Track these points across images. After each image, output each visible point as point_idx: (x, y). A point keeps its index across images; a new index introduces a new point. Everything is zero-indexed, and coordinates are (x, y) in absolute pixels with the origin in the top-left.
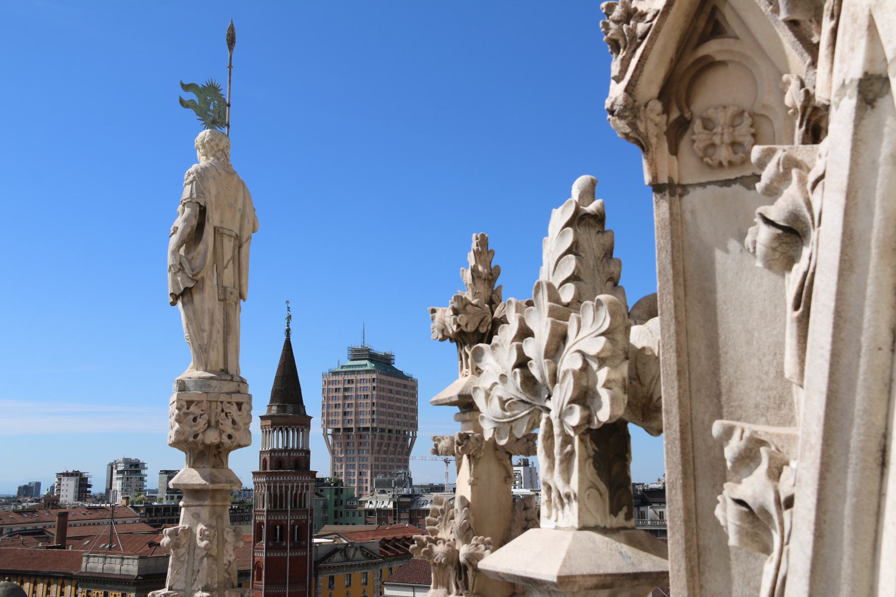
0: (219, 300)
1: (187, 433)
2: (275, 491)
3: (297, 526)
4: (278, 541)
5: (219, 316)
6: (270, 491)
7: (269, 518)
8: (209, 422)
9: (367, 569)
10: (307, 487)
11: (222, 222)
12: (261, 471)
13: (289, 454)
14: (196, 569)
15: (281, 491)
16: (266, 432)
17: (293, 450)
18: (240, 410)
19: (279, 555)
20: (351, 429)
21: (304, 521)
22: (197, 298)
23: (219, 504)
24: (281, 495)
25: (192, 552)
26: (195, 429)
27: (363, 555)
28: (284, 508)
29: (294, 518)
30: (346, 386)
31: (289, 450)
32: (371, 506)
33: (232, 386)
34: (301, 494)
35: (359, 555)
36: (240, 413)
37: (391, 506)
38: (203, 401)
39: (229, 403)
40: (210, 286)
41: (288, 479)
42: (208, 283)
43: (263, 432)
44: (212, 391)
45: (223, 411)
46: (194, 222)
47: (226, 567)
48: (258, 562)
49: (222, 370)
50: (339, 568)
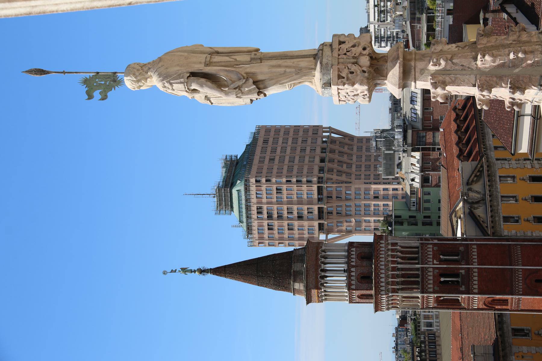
0: (261, 62)
1: (362, 78)
2: (397, 283)
3: (441, 257)
4: (459, 279)
5: (274, 62)
6: (398, 289)
7: (431, 290)
8: (353, 63)
9: (495, 176)
10: (394, 244)
11: (201, 63)
12: (373, 301)
13: (353, 266)
14: (461, 68)
15: (398, 276)
16: (326, 295)
17: (348, 263)
18: (344, 42)
19: (476, 278)
20: (320, 210)
21: (435, 248)
22: (260, 77)
23: (414, 56)
24: (403, 276)
25: (449, 72)
26: (359, 72)
27: (477, 181)
28: (419, 273)
29: (431, 260)
30: (265, 216)
31: (348, 266)
32: (418, 179)
33: (327, 51)
34: (402, 252)
35: (477, 187)
36: (347, 42)
37: (417, 155)
38: (338, 68)
39: (339, 50)
40: (249, 68)
41: (383, 267)
42: (248, 70)
43: (326, 299)
44: (330, 62)
45: (345, 54)
46: (203, 80)
47: (460, 49)
48: (485, 305)
49: (315, 58)
50: (494, 211)
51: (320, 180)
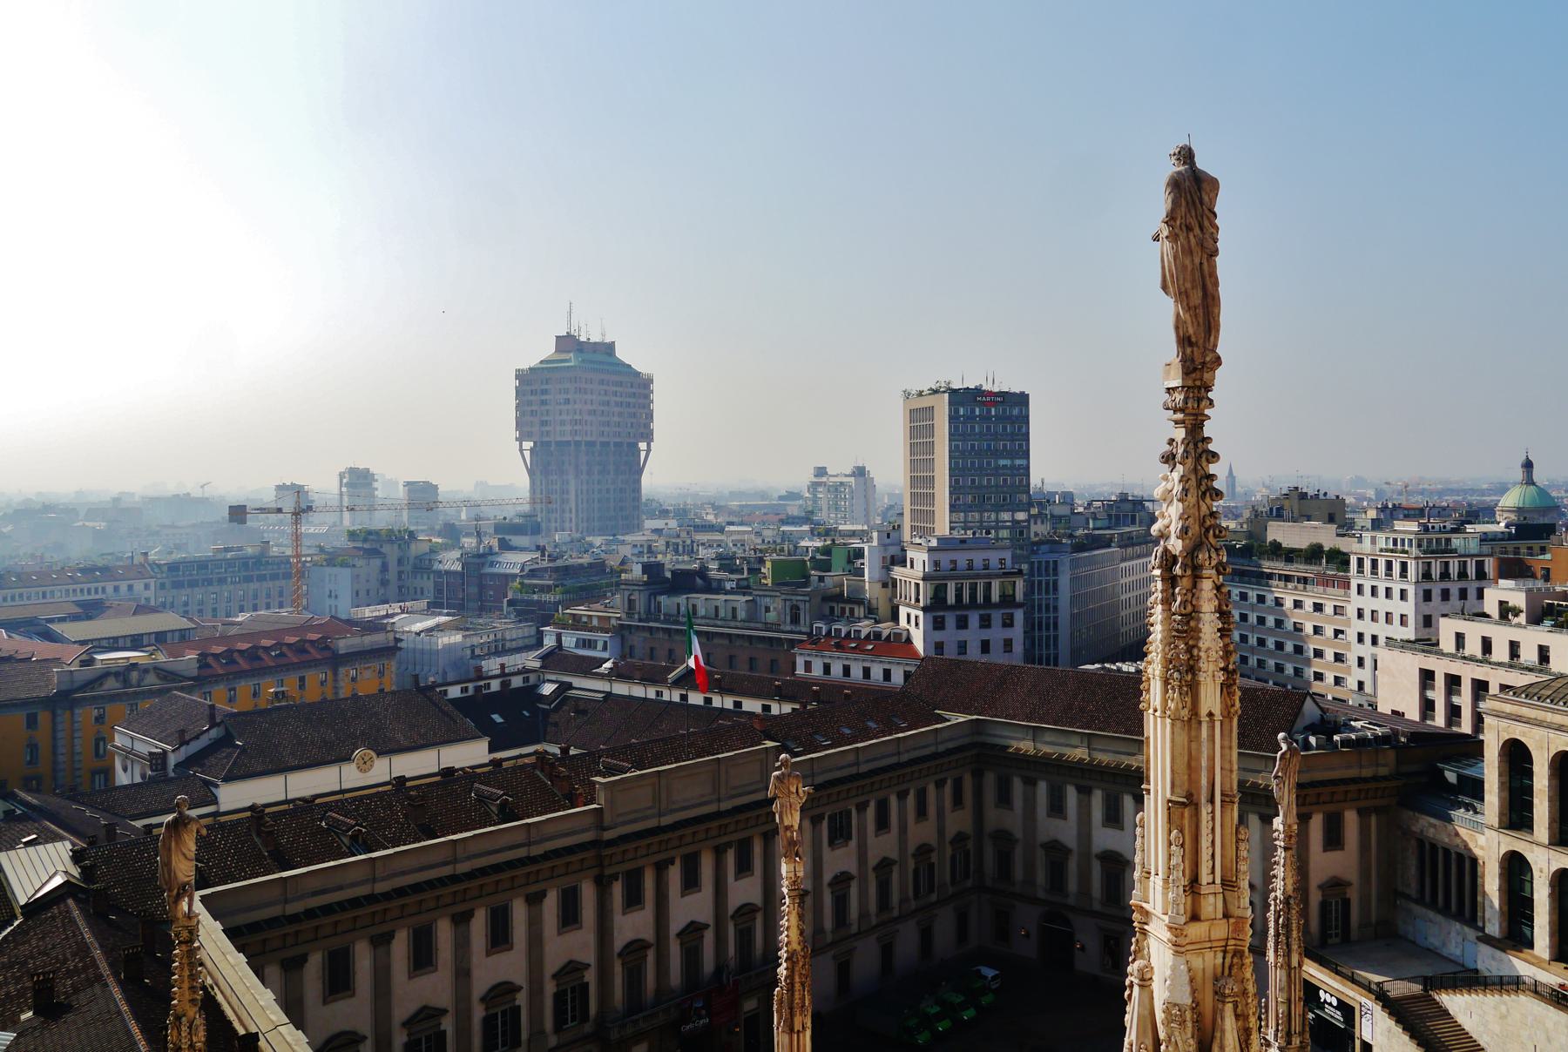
20: (548, 444)
27: (158, 676)
32: (441, 567)
35: (151, 679)
37: (460, 569)
50: (113, 698)
51: (578, 444)
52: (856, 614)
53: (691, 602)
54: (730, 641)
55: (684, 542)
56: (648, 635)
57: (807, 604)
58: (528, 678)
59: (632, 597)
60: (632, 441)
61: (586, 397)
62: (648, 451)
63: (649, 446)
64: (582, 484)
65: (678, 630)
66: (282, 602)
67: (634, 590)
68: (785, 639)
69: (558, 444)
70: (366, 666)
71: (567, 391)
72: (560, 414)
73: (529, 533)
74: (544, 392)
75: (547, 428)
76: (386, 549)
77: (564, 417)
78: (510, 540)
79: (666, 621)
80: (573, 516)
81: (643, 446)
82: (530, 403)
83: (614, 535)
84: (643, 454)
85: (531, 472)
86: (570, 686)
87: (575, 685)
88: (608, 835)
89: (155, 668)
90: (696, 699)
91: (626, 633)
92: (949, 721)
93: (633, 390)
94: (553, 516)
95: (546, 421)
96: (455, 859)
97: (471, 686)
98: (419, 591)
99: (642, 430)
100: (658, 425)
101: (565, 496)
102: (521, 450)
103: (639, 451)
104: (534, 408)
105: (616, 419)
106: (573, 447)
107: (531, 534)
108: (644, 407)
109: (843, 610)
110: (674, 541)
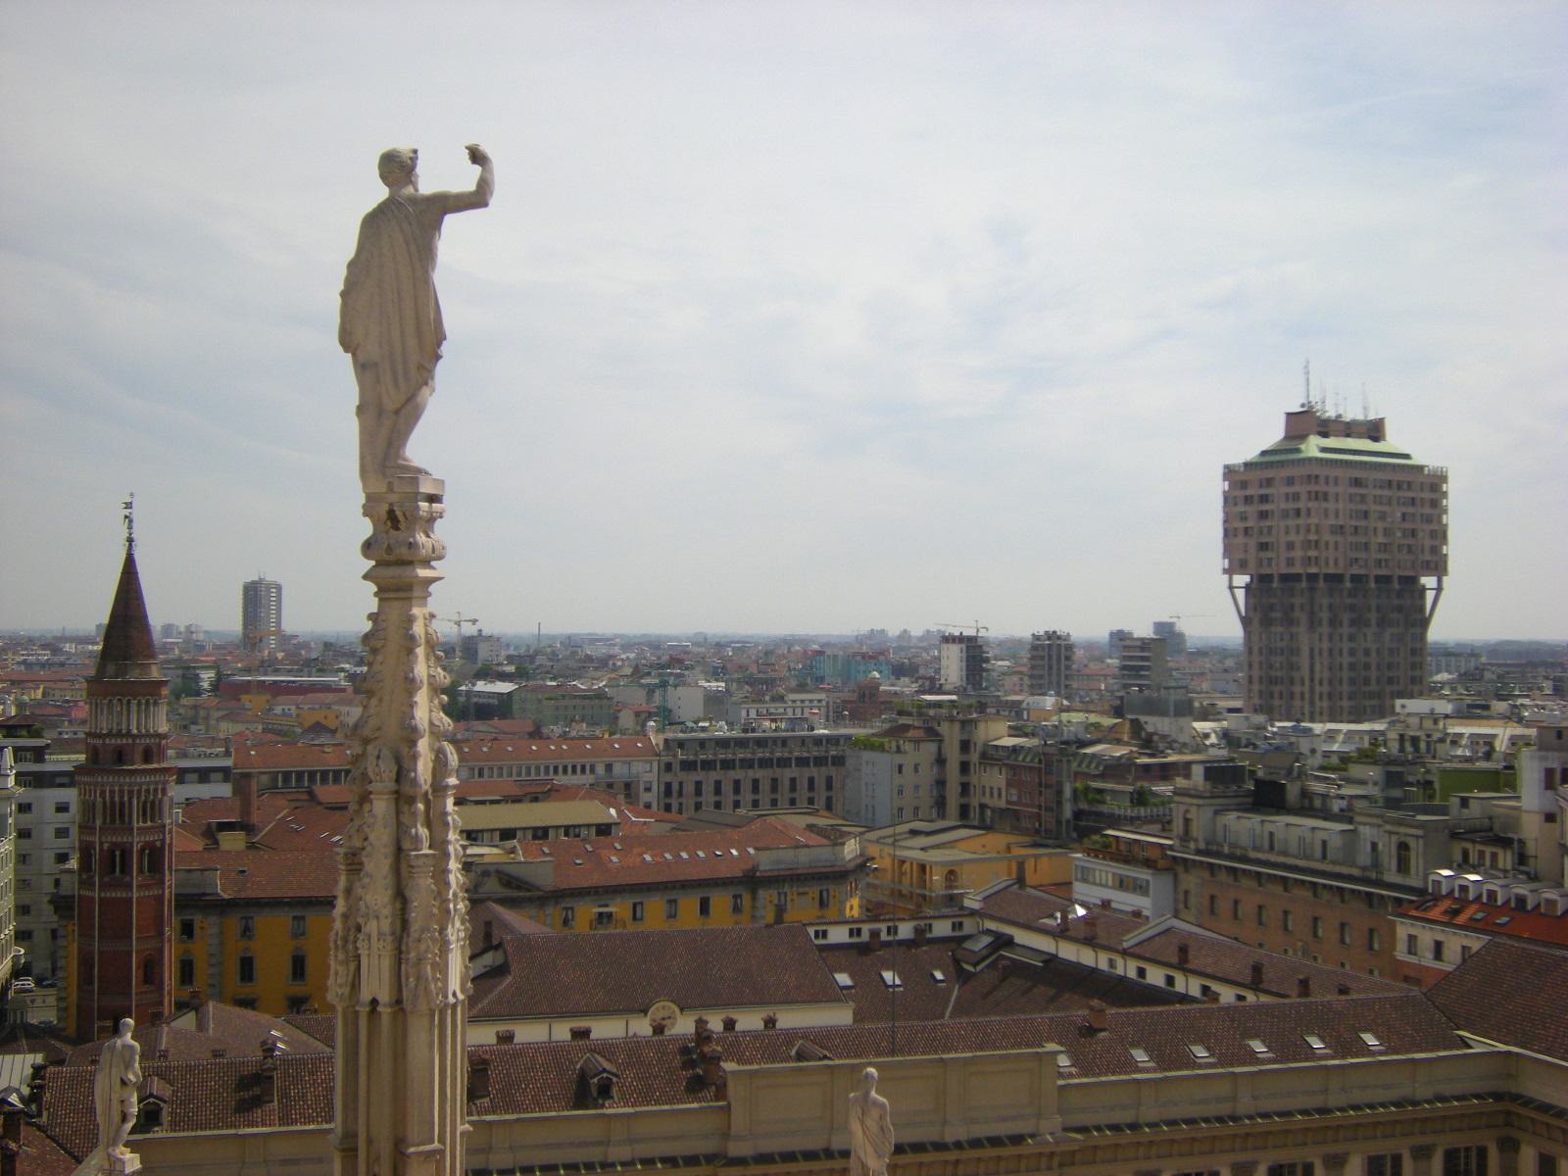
3: (147, 852)
6: (104, 798)
20: (1271, 576)
24: (122, 804)
34: (153, 802)
51: (1312, 577)
52: (1501, 865)
53: (1269, 827)
54: (1315, 895)
55: (1429, 736)
56: (1206, 875)
57: (1421, 841)
58: (961, 924)
59: (1189, 816)
60: (1412, 574)
61: (1324, 505)
62: (1439, 589)
63: (1440, 582)
64: (1320, 640)
65: (1244, 870)
66: (758, 800)
67: (1192, 804)
68: (1389, 897)
69: (1285, 578)
70: (801, 890)
71: (1296, 497)
72: (1287, 533)
73: (1172, 714)
74: (1264, 499)
75: (1270, 554)
76: (944, 729)
77: (1292, 537)
78: (1146, 723)
79: (1231, 857)
80: (1306, 688)
81: (1428, 581)
82: (1243, 517)
83: (1298, 721)
84: (1430, 596)
85: (1246, 621)
86: (1008, 942)
87: (1017, 940)
88: (735, 1149)
89: (498, 872)
90: (1156, 977)
91: (1180, 869)
92: (1470, 1047)
93: (1411, 494)
94: (1276, 689)
95: (1267, 543)
96: (491, 1148)
97: (866, 928)
98: (988, 790)
99: (1427, 557)
100: (1455, 549)
101: (1294, 659)
102: (1231, 588)
103: (1424, 589)
104: (1249, 524)
105: (1381, 539)
106: (1304, 584)
107: (1175, 715)
108: (1429, 519)
109: (1482, 854)
110: (1411, 733)
